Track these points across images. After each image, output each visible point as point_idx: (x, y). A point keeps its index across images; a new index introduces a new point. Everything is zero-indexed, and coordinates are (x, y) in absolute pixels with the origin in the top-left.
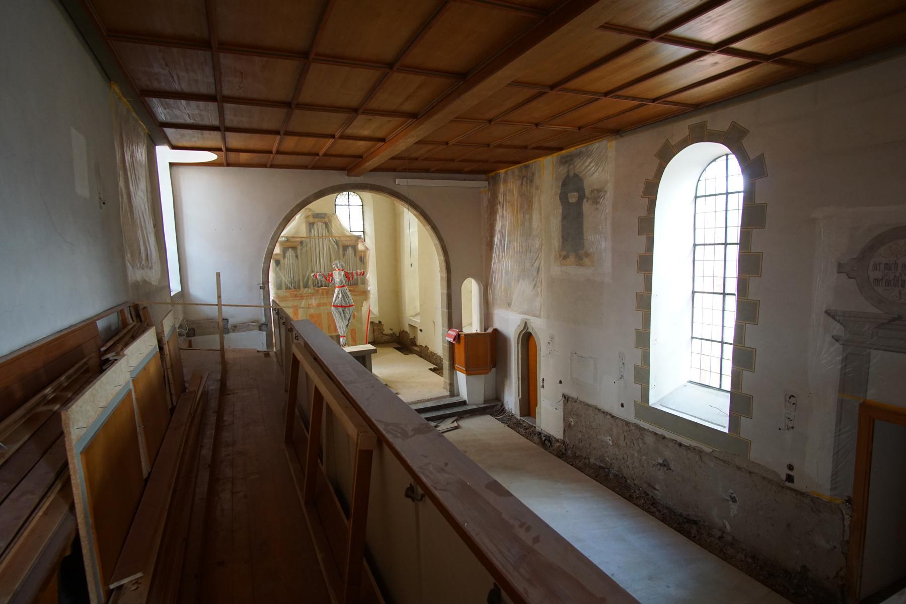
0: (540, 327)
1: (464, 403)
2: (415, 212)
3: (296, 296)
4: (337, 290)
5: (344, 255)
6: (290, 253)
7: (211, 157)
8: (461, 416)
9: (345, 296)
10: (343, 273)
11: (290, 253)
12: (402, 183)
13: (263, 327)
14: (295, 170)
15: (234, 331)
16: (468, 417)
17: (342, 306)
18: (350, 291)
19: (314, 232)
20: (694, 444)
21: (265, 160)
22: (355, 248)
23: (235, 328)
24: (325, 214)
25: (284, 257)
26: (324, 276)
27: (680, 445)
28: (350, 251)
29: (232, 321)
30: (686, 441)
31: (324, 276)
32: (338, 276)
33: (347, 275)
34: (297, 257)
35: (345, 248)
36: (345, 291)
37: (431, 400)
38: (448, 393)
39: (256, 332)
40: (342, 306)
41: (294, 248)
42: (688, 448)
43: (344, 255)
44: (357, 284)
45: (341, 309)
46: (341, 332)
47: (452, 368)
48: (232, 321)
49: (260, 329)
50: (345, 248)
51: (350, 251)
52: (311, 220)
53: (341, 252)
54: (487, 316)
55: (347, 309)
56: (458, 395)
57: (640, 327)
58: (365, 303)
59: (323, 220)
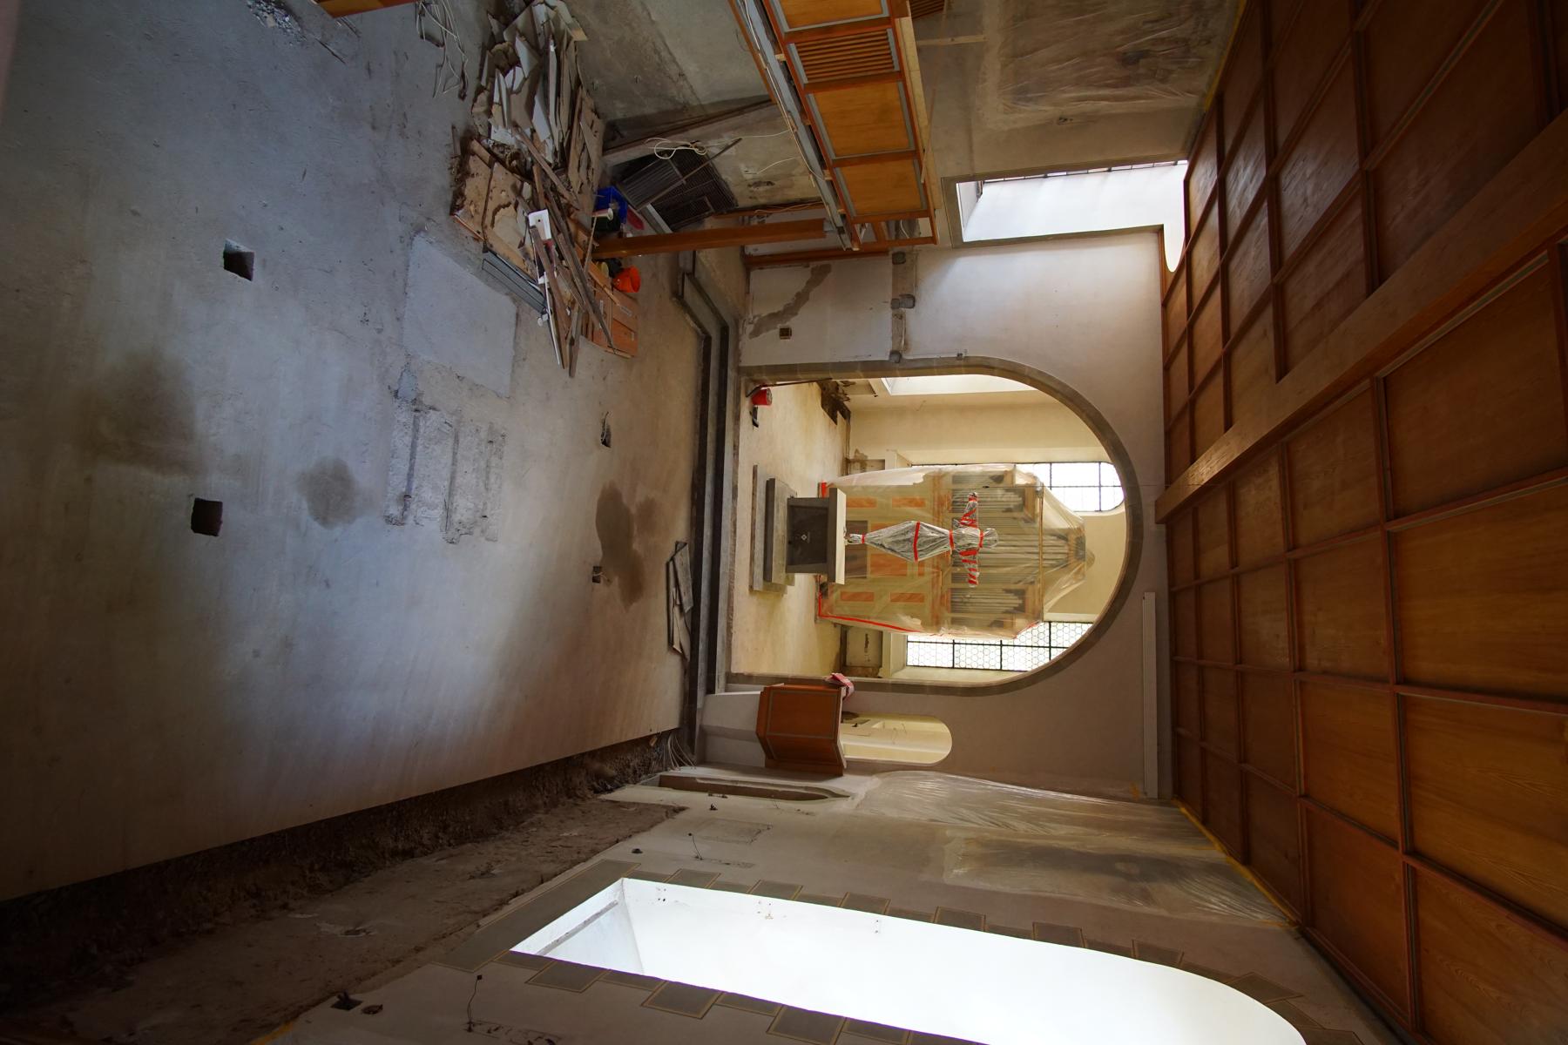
0: (841, 806)
1: (710, 690)
3: (941, 504)
4: (947, 532)
5: (1008, 591)
6: (1014, 499)
7: (1173, 264)
8: (689, 671)
9: (935, 543)
10: (976, 543)
11: (1014, 499)
13: (896, 358)
14: (1161, 401)
15: (894, 315)
16: (683, 684)
17: (916, 537)
18: (941, 556)
19: (1050, 540)
20: (508, 910)
21: (1177, 342)
22: (1020, 610)
23: (899, 317)
26: (972, 512)
27: (516, 895)
28: (1015, 601)
29: (909, 313)
30: (515, 904)
31: (972, 512)
32: (971, 533)
33: (971, 551)
34: (1009, 510)
35: (1021, 593)
36: (942, 544)
37: (729, 627)
38: (734, 670)
39: (889, 346)
40: (916, 537)
41: (1023, 506)
42: (503, 903)
43: (1008, 591)
44: (953, 611)
45: (911, 535)
48: (909, 313)
49: (893, 353)
50: (1021, 593)
51: (1015, 601)
52: (1072, 537)
53: (1013, 587)
54: (866, 768)
55: (910, 546)
57: (804, 892)
58: (918, 622)
59: (1073, 560)
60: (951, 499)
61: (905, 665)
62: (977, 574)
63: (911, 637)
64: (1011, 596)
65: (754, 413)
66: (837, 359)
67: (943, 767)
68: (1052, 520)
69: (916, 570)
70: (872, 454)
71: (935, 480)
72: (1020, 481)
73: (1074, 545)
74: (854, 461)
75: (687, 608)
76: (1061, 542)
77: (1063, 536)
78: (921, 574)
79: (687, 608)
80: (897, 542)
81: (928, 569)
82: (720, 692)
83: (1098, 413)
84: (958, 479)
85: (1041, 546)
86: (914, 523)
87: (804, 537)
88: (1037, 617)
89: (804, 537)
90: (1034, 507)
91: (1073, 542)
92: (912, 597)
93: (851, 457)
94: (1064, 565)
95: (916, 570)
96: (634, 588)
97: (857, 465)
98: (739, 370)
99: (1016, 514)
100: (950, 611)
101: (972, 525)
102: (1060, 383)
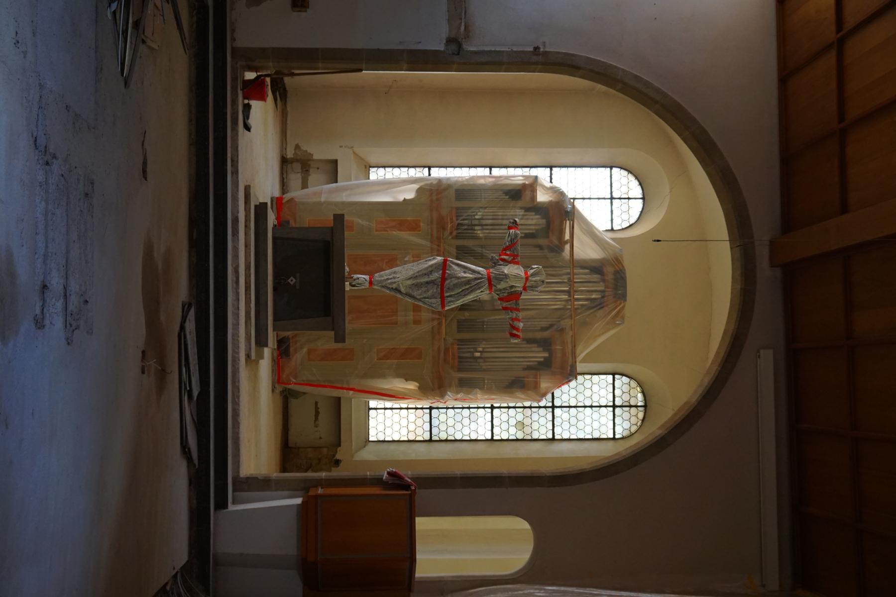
1: (222, 504)
2: (694, 400)
3: (442, 226)
5: (529, 341)
6: (534, 221)
9: (469, 286)
10: (519, 285)
12: (764, 365)
13: (453, 47)
17: (443, 278)
19: (581, 275)
22: (546, 365)
24: (623, 297)
25: (527, 210)
28: (540, 355)
33: (512, 297)
36: (478, 287)
39: (444, 31)
44: (460, 370)
45: (436, 275)
46: (384, 275)
47: (305, 487)
49: (450, 41)
50: (545, 344)
51: (540, 355)
52: (609, 270)
53: (539, 335)
55: (434, 290)
56: (234, 503)
58: (412, 386)
60: (447, 216)
61: (368, 441)
62: (521, 325)
63: (373, 404)
64: (534, 347)
65: (247, 107)
66: (373, 45)
67: (530, 575)
68: (585, 250)
69: (411, 316)
70: (320, 152)
71: (434, 192)
72: (542, 197)
73: (610, 276)
74: (292, 161)
75: (195, 393)
76: (596, 277)
77: (596, 268)
78: (417, 322)
79: (195, 393)
80: (418, 286)
81: (425, 315)
82: (231, 507)
83: (704, 132)
84: (465, 192)
85: (571, 282)
86: (439, 259)
87: (292, 281)
88: (569, 374)
89: (292, 281)
90: (562, 232)
91: (610, 277)
93: (290, 154)
94: (598, 305)
95: (411, 316)
96: (162, 374)
97: (297, 166)
98: (233, 49)
99: (542, 241)
100: (446, 373)
101: (514, 262)
102: (658, 91)
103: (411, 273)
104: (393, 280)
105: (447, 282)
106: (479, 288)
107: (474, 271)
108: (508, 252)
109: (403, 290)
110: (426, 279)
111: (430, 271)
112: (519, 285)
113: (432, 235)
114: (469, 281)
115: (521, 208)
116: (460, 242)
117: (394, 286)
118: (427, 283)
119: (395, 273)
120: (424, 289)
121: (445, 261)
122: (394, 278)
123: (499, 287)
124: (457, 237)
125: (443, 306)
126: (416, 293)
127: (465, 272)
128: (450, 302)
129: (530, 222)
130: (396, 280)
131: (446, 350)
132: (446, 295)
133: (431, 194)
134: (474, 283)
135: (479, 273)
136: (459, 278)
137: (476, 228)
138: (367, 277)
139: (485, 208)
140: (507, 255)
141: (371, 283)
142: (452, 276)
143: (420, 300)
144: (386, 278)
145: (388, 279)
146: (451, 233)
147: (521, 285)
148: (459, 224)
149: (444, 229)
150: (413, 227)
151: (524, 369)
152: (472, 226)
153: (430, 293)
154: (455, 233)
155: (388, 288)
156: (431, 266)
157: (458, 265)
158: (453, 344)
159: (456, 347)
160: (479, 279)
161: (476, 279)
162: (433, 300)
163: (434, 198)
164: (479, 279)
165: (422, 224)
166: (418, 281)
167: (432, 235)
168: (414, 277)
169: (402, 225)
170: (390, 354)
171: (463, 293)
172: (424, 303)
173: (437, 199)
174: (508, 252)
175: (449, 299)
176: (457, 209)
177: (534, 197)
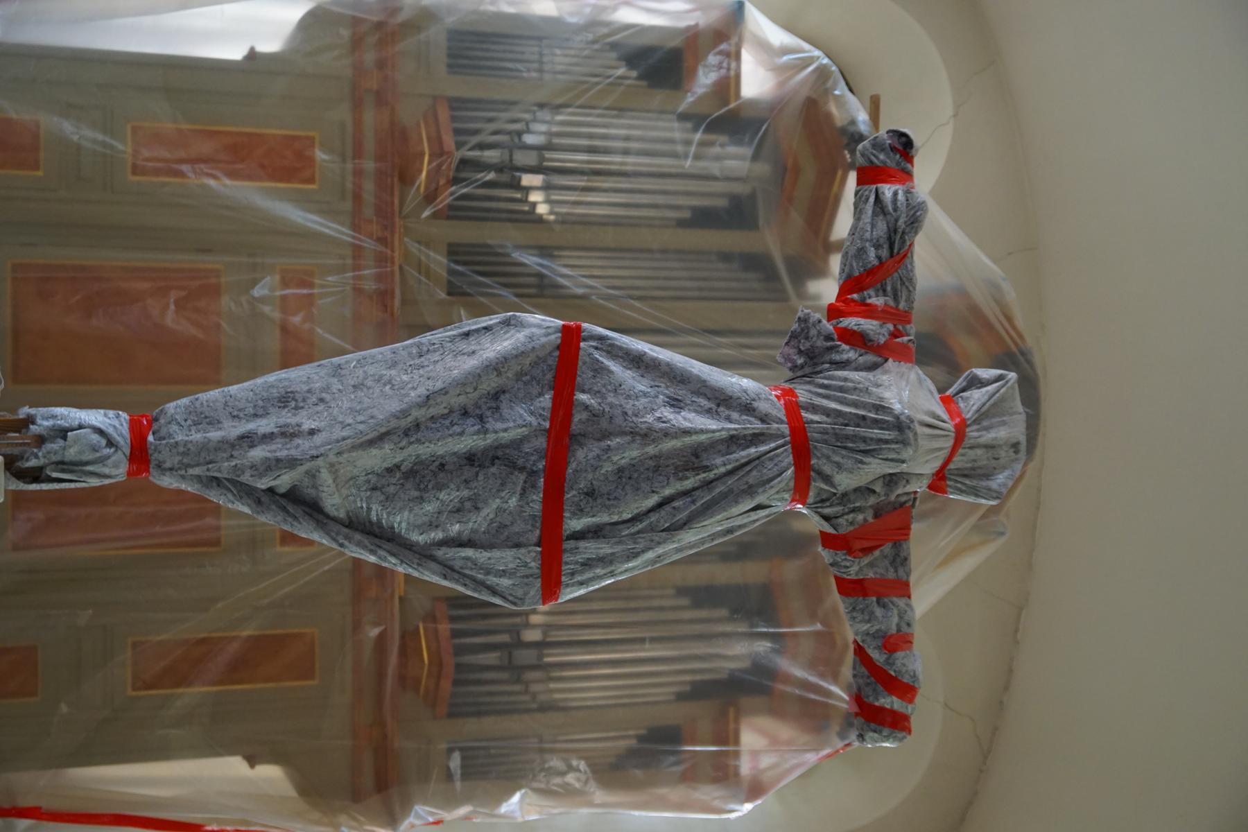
5: (704, 596)
17: (561, 434)
36: (743, 483)
45: (524, 419)
55: (513, 503)
80: (419, 477)
86: (539, 326)
92: (261, 656)
103: (385, 406)
104: (280, 450)
105: (581, 456)
106: (750, 491)
107: (722, 401)
108: (878, 301)
109: (333, 502)
110: (469, 441)
111: (485, 397)
112: (922, 463)
113: (357, 198)
114: (695, 457)
115: (683, 117)
116: (467, 233)
117: (284, 481)
118: (471, 458)
119: (286, 400)
120: (450, 496)
121: (571, 337)
122: (288, 434)
123: (845, 482)
124: (454, 213)
125: (551, 587)
126: (400, 521)
127: (676, 403)
128: (587, 564)
129: (714, 168)
130: (303, 446)
131: (409, 639)
132: (574, 524)
133: (356, 43)
134: (720, 464)
135: (747, 408)
136: (647, 436)
137: (527, 180)
138: (112, 421)
139: (558, 108)
140: (868, 311)
141: (140, 456)
142: (606, 427)
143: (424, 555)
144: (233, 430)
145: (249, 440)
146: (430, 198)
147: (929, 467)
148: (464, 163)
149: (406, 178)
150: (285, 163)
151: (681, 697)
152: (509, 174)
153: (479, 522)
154: (445, 199)
155: (246, 492)
156: (497, 366)
157: (637, 362)
158: (431, 617)
159: (444, 628)
160: (756, 438)
161: (734, 441)
162: (505, 558)
163: (370, 57)
164: (756, 438)
165: (320, 155)
166: (424, 450)
167: (357, 198)
168: (408, 429)
169: (242, 154)
170: (183, 666)
171: (662, 518)
172: (448, 570)
173: (381, 65)
174: (878, 301)
175: (590, 548)
176: (457, 104)
177: (728, 85)
